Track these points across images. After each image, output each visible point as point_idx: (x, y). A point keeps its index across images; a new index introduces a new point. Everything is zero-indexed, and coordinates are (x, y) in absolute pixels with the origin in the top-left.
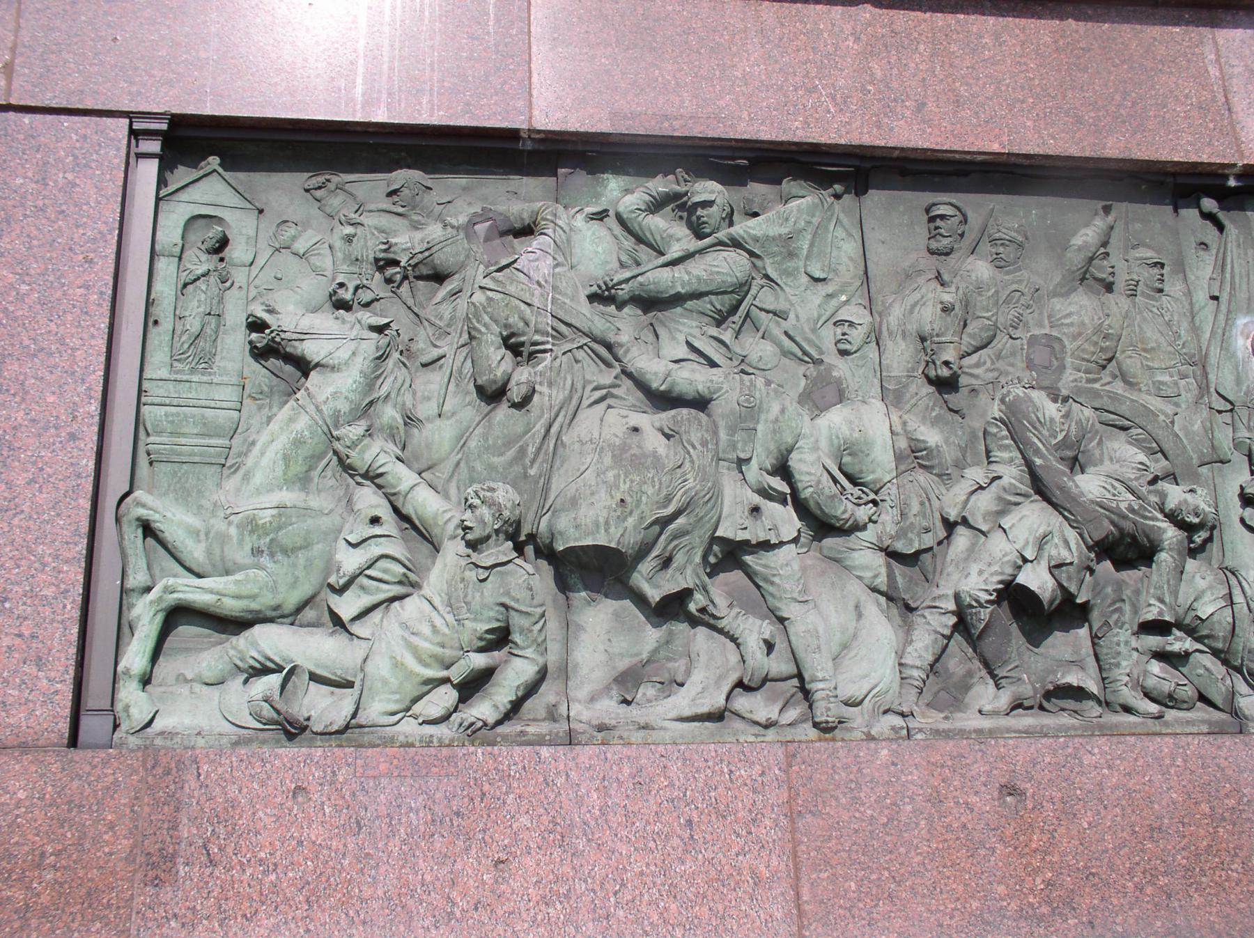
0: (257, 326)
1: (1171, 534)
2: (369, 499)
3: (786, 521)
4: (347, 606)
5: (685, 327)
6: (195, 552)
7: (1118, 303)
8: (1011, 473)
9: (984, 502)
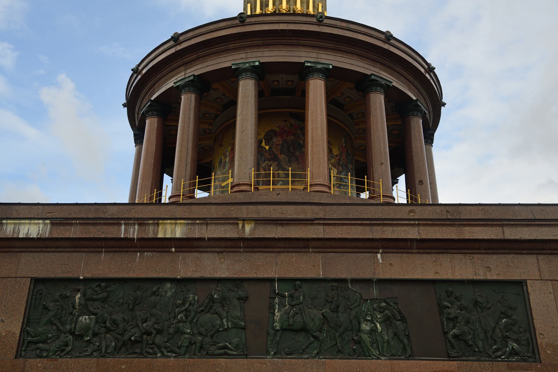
0: (44, 305)
1: (154, 332)
2: (54, 327)
3: (103, 330)
4: (49, 341)
5: (97, 304)
6: (33, 334)
7: (158, 297)
8: (134, 323)
9: (130, 327)
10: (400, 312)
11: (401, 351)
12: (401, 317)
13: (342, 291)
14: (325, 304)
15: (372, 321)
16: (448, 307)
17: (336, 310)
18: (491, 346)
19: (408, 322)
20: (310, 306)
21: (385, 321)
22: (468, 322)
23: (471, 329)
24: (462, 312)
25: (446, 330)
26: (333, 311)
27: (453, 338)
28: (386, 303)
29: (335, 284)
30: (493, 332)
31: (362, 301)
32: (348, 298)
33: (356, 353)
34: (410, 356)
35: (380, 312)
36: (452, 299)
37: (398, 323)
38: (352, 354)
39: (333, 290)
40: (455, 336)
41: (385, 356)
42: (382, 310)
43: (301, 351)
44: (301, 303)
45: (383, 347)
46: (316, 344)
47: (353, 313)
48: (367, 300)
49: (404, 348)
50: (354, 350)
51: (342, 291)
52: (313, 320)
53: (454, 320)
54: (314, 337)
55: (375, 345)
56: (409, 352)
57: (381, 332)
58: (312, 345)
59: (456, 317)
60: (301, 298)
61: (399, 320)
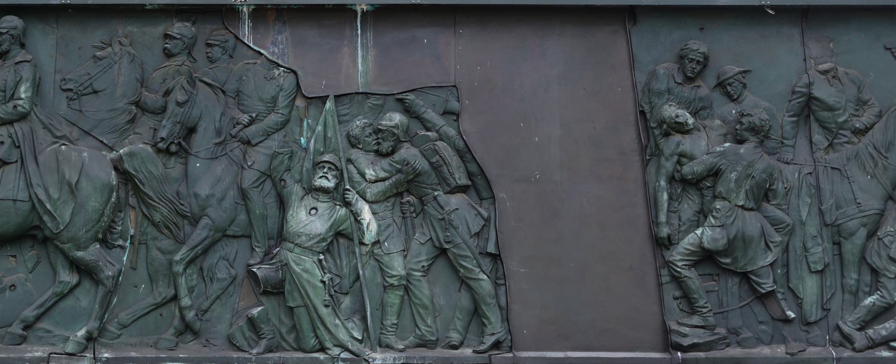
10: (465, 153)
11: (459, 325)
12: (470, 175)
13: (211, 60)
14: (132, 121)
15: (338, 195)
16: (681, 128)
17: (178, 147)
18: (856, 295)
19: (500, 195)
20: (65, 130)
21: (400, 195)
22: (763, 194)
23: (775, 223)
24: (742, 149)
25: (665, 231)
26: (167, 152)
27: (695, 265)
28: (408, 110)
29: (179, 28)
30: (871, 235)
31: (300, 103)
32: (238, 93)
33: (260, 337)
34: (497, 345)
35: (378, 153)
36: (704, 91)
37: (456, 200)
38: (240, 341)
39: (168, 54)
40: (705, 258)
41: (389, 347)
42: (386, 146)
43: (17, 329)
44: (23, 117)
45: (382, 307)
46: (86, 298)
47: (258, 157)
48: (323, 99)
49: (476, 313)
50: (251, 321)
51: (211, 60)
52: (73, 190)
53: (702, 184)
54: (76, 266)
55: (346, 302)
56: (495, 328)
57: (377, 242)
58: (69, 302)
59: (715, 174)
60: (24, 91)
61: (463, 189)
